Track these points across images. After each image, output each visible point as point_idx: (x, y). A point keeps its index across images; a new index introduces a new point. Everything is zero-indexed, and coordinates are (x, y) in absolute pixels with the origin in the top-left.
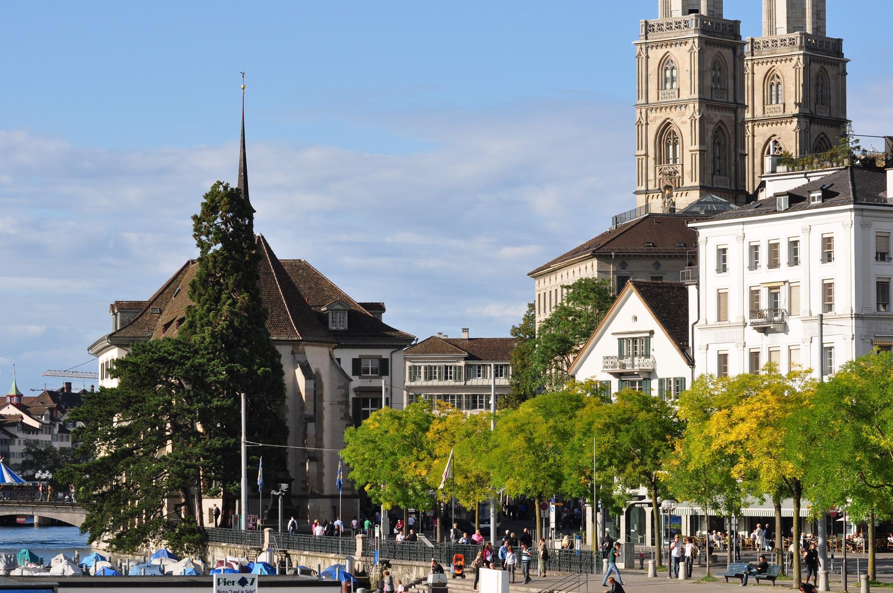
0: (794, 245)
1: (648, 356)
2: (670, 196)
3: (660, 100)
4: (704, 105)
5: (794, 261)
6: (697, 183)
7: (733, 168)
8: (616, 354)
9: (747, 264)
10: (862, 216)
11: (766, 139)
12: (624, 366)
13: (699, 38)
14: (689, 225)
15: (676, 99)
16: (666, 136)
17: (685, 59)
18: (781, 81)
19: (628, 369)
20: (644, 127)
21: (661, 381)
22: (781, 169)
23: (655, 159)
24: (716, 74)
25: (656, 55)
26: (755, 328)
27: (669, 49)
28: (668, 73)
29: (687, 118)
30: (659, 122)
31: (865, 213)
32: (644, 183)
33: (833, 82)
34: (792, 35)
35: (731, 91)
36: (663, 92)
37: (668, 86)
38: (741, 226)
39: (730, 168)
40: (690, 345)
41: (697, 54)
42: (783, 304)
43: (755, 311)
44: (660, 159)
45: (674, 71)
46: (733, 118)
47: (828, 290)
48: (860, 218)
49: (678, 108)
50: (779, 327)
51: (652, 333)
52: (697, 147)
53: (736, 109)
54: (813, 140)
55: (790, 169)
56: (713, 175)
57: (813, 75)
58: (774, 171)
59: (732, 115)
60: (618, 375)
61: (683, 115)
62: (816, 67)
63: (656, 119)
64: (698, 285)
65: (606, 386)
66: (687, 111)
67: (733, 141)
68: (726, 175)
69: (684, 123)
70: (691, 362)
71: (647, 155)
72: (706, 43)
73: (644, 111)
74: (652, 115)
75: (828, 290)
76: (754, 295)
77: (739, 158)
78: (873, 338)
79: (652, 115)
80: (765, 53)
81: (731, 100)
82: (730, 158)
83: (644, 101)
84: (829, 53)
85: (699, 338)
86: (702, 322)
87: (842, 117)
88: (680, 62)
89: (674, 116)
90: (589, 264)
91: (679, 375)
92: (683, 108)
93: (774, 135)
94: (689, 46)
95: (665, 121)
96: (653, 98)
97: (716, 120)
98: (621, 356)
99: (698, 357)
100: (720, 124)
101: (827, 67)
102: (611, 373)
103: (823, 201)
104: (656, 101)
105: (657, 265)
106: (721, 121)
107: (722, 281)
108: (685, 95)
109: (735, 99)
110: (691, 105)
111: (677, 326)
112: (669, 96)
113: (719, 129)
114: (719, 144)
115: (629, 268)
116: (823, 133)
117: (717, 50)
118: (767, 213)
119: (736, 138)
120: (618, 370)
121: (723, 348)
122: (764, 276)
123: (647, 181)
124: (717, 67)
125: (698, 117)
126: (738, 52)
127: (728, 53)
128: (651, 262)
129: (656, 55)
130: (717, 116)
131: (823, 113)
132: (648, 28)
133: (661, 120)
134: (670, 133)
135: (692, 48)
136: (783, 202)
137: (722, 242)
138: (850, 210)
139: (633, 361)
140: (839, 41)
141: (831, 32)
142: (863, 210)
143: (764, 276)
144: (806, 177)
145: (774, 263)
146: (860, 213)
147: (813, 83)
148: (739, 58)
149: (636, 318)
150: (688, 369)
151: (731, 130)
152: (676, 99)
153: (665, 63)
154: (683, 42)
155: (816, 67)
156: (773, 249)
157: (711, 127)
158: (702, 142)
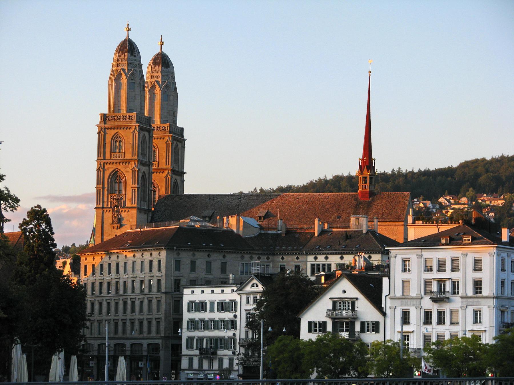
1: (353, 309)
2: (118, 211)
3: (112, 158)
5: (455, 268)
6: (135, 205)
8: (332, 309)
9: (423, 268)
15: (123, 158)
16: (116, 177)
17: (129, 138)
18: (156, 149)
19: (340, 316)
20: (102, 172)
21: (362, 324)
22: (417, 222)
23: (108, 190)
27: (119, 130)
28: (117, 144)
30: (111, 170)
32: (101, 203)
33: (180, 151)
34: (164, 125)
36: (114, 154)
37: (117, 151)
38: (420, 251)
40: (383, 305)
41: (137, 135)
43: (428, 291)
44: (112, 190)
45: (122, 144)
49: (124, 164)
50: (447, 300)
51: (357, 299)
52: (136, 185)
58: (414, 223)
60: (333, 319)
61: (127, 167)
62: (175, 142)
63: (110, 168)
65: (325, 323)
66: (130, 165)
68: (144, 201)
70: (384, 314)
71: (103, 188)
73: (102, 163)
74: (107, 166)
76: (427, 283)
81: (147, 160)
83: (102, 158)
84: (178, 135)
85: (388, 304)
86: (392, 295)
89: (121, 167)
90: (155, 254)
91: (375, 320)
92: (127, 164)
94: (132, 130)
95: (115, 170)
96: (108, 156)
97: (142, 171)
99: (388, 312)
101: (178, 143)
102: (332, 318)
103: (472, 241)
105: (194, 255)
106: (144, 172)
107: (406, 276)
108: (128, 156)
111: (375, 298)
112: (117, 156)
115: (180, 256)
117: (144, 132)
120: (334, 316)
121: (405, 308)
123: (103, 202)
125: (137, 169)
127: (147, 134)
128: (191, 253)
129: (111, 133)
130: (144, 169)
131: (176, 169)
132: (104, 118)
133: (113, 169)
135: (134, 131)
137: (406, 257)
139: (342, 312)
140: (183, 129)
141: (180, 124)
143: (435, 275)
148: (151, 137)
149: (344, 292)
150: (383, 318)
151: (147, 177)
152: (123, 158)
157: (141, 175)
158: (138, 184)
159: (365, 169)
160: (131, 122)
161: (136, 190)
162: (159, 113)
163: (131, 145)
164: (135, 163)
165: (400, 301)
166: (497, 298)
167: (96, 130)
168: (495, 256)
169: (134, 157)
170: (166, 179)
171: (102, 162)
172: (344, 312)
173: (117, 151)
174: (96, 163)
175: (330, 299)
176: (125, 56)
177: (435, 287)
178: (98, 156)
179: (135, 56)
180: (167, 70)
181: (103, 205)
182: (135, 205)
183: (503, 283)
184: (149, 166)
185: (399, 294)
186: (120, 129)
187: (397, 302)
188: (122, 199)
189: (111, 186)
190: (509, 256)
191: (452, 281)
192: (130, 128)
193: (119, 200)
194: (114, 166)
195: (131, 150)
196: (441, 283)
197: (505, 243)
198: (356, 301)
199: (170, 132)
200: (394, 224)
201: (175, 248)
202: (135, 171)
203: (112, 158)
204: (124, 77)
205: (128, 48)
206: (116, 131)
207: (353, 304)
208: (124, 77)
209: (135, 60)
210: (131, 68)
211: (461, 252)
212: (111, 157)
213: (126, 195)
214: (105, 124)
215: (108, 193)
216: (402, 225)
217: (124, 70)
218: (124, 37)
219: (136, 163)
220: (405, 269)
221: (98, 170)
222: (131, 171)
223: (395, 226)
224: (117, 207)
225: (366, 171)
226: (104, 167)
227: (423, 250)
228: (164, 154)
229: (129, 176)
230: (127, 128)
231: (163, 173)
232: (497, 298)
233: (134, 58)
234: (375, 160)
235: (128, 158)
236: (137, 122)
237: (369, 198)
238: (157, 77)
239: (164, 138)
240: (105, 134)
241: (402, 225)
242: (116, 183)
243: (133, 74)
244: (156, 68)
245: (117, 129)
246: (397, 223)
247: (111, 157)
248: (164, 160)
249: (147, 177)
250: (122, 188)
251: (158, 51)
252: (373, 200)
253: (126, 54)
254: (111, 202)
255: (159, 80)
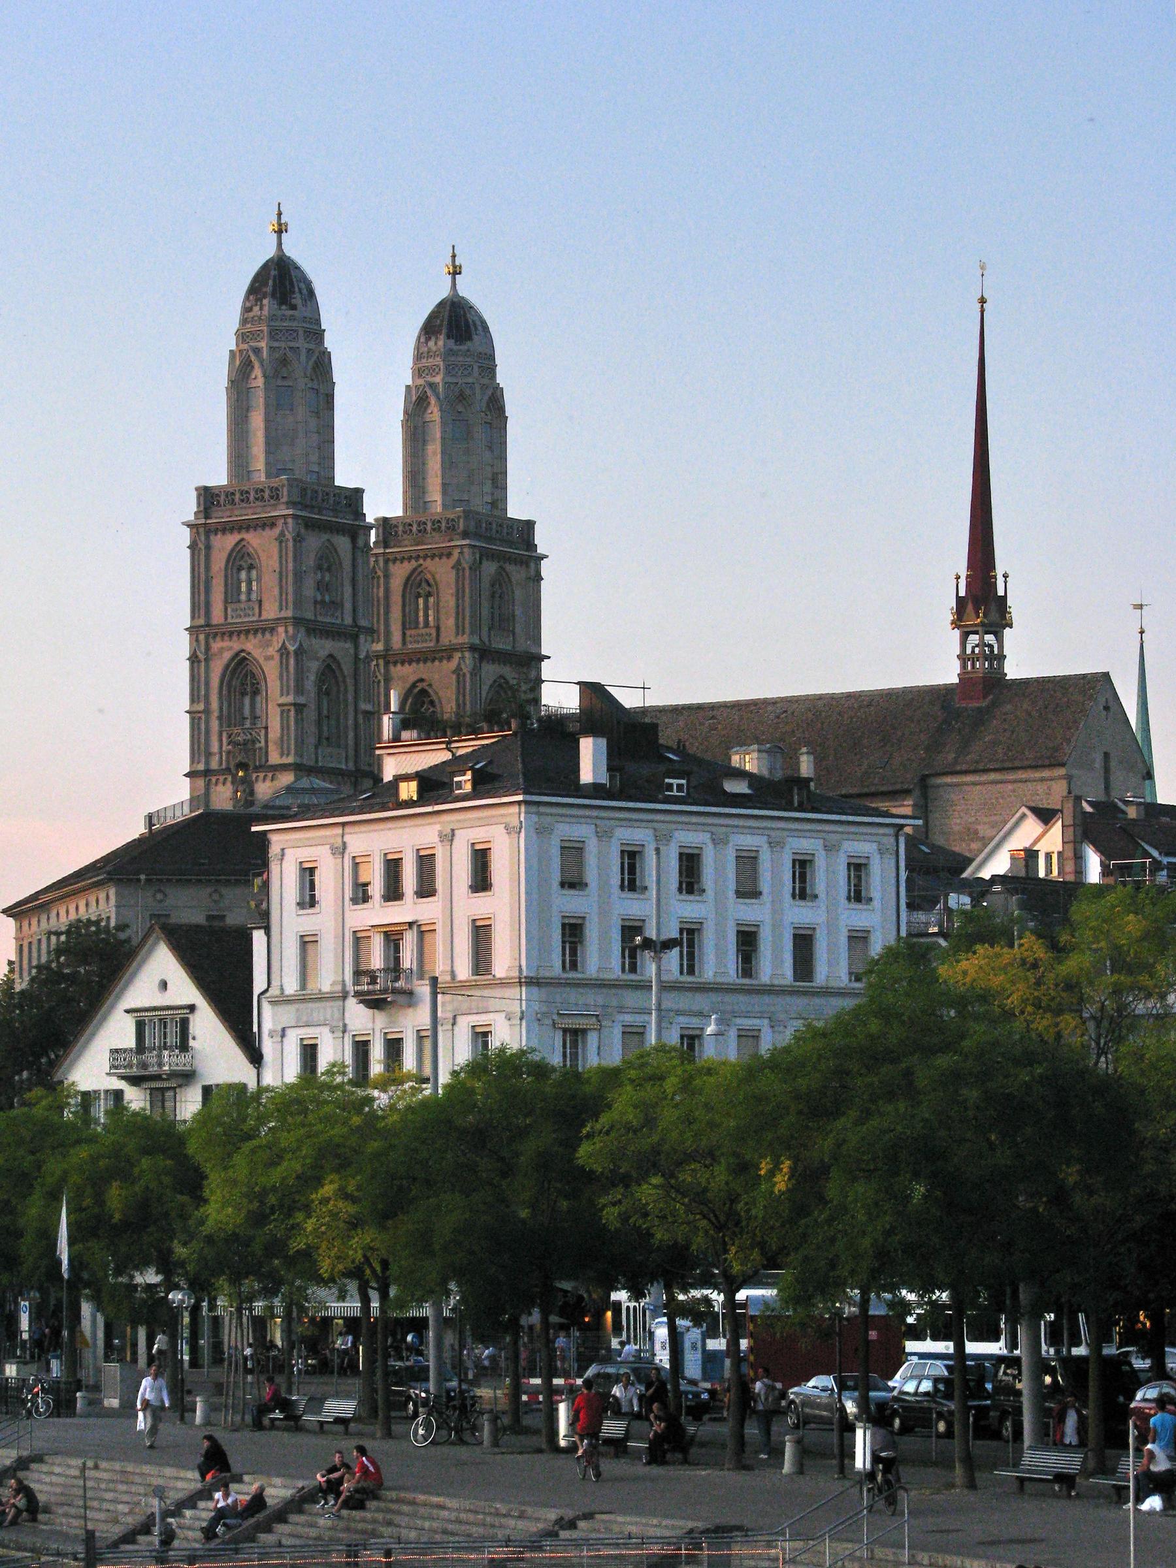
0: (426, 863)
1: (184, 1047)
3: (230, 620)
4: (302, 630)
7: (351, 735)
8: (132, 1043)
9: (348, 894)
10: (539, 814)
11: (408, 686)
12: (144, 1066)
13: (295, 517)
14: (254, 829)
15: (255, 619)
16: (241, 679)
19: (154, 1070)
21: (207, 1091)
22: (405, 735)
23: (220, 718)
24: (323, 577)
25: (224, 544)
26: (361, 1002)
27: (244, 535)
29: (272, 651)
30: (227, 655)
31: (542, 809)
33: (518, 593)
35: (348, 606)
36: (233, 606)
37: (243, 597)
38: (339, 831)
39: (346, 733)
40: (255, 1029)
41: (291, 544)
42: (408, 959)
44: (232, 718)
45: (254, 573)
46: (352, 651)
47: (481, 934)
48: (535, 818)
49: (259, 635)
50: (401, 999)
51: (192, 1008)
53: (357, 636)
54: (485, 688)
55: (423, 736)
56: (316, 747)
57: (486, 583)
58: (396, 738)
59: (349, 645)
61: (268, 644)
62: (490, 568)
63: (225, 650)
64: (268, 930)
66: (275, 638)
67: (351, 689)
68: (339, 747)
69: (268, 658)
70: (256, 1058)
71: (207, 711)
72: (307, 526)
73: (202, 637)
75: (481, 934)
77: (360, 717)
78: (555, 1017)
79: (216, 645)
80: (406, 542)
81: (348, 620)
82: (346, 719)
84: (511, 544)
85: (268, 1019)
87: (533, 650)
88: (263, 556)
89: (252, 645)
92: (268, 635)
93: (422, 680)
95: (237, 654)
96: (217, 616)
97: (323, 654)
98: (141, 1047)
99: (268, 1047)
100: (329, 661)
101: (510, 568)
104: (222, 621)
106: (331, 656)
107: (307, 922)
109: (354, 620)
110: (281, 630)
113: (330, 669)
114: (328, 693)
115: (169, 902)
116: (501, 677)
118: (384, 809)
119: (356, 685)
120: (135, 1071)
122: (379, 913)
123: (209, 755)
124: (325, 566)
126: (360, 543)
127: (343, 543)
128: (204, 893)
129: (224, 544)
130: (324, 647)
131: (501, 643)
132: (208, 497)
134: (246, 676)
135: (282, 534)
136: (408, 790)
138: (519, 803)
139: (160, 1056)
140: (529, 525)
142: (538, 803)
143: (379, 913)
144: (449, 749)
145: (393, 893)
146: (534, 809)
147: (486, 594)
149: (164, 985)
151: (347, 668)
153: (240, 560)
154: (270, 523)
155: (490, 568)
156: (393, 867)
157: (314, 666)
159: (970, 607)
160: (275, 507)
161: (292, 713)
162: (439, 481)
163: (277, 575)
164: (286, 632)
165: (291, 1009)
166: (531, 982)
167: (186, 535)
168: (523, 834)
169: (283, 614)
170: (458, 675)
171: (203, 631)
172: (166, 1053)
173: (243, 597)
174: (186, 637)
175: (127, 1011)
176: (261, 309)
177: (376, 960)
178: (193, 618)
179: (294, 307)
180: (463, 348)
181: (207, 763)
182: (290, 760)
183: (573, 932)
184: (355, 638)
185: (291, 986)
186: (248, 529)
187: (287, 1015)
188: (254, 741)
189: (230, 705)
190: (662, 838)
191: (421, 933)
192: (273, 525)
193: (248, 746)
194: (235, 645)
195: (276, 591)
196: (392, 937)
197: (596, 790)
198: (190, 1016)
199: (465, 535)
200: (1038, 775)
201: (143, 877)
202: (288, 653)
203: (230, 620)
204: (257, 372)
205: (281, 288)
206: (236, 537)
207: (184, 1024)
208: (257, 372)
209: (292, 318)
210: (276, 344)
211: (438, 827)
212: (226, 619)
213: (266, 728)
214: (206, 518)
215: (221, 725)
216: (1061, 777)
217: (257, 351)
218: (270, 252)
219: (290, 629)
220: (309, 901)
221: (193, 659)
222: (277, 656)
223: (1042, 780)
224: (242, 766)
225: (973, 615)
226: (208, 648)
227: (348, 829)
228: (452, 603)
229: (271, 671)
230: (264, 526)
231: (449, 658)
232: (531, 982)
233: (291, 312)
234: (1006, 576)
235: (272, 616)
236: (291, 504)
237: (985, 697)
238: (432, 370)
239: (449, 555)
240: (208, 547)
241: (1061, 777)
242: (243, 694)
243: (284, 362)
244: (431, 344)
245: (240, 530)
246: (1046, 773)
247: (226, 619)
248: (451, 622)
249: (347, 668)
250: (258, 713)
251: (444, 292)
252: (994, 704)
253: (265, 302)
254: (229, 752)
255: (438, 379)
